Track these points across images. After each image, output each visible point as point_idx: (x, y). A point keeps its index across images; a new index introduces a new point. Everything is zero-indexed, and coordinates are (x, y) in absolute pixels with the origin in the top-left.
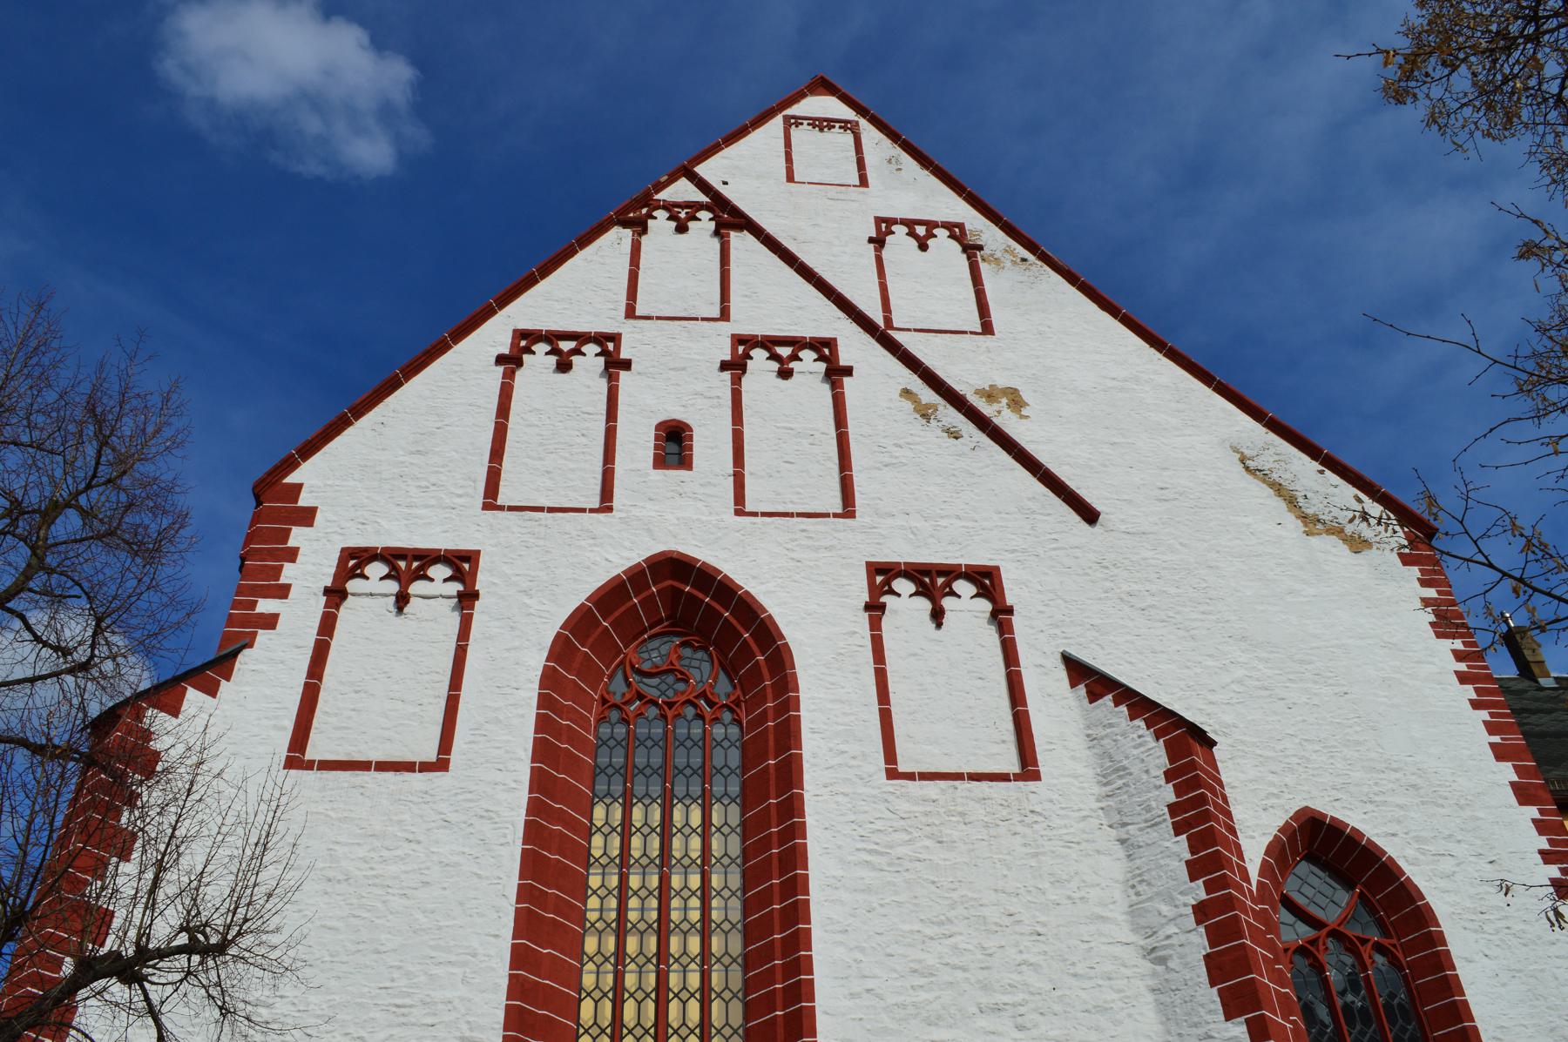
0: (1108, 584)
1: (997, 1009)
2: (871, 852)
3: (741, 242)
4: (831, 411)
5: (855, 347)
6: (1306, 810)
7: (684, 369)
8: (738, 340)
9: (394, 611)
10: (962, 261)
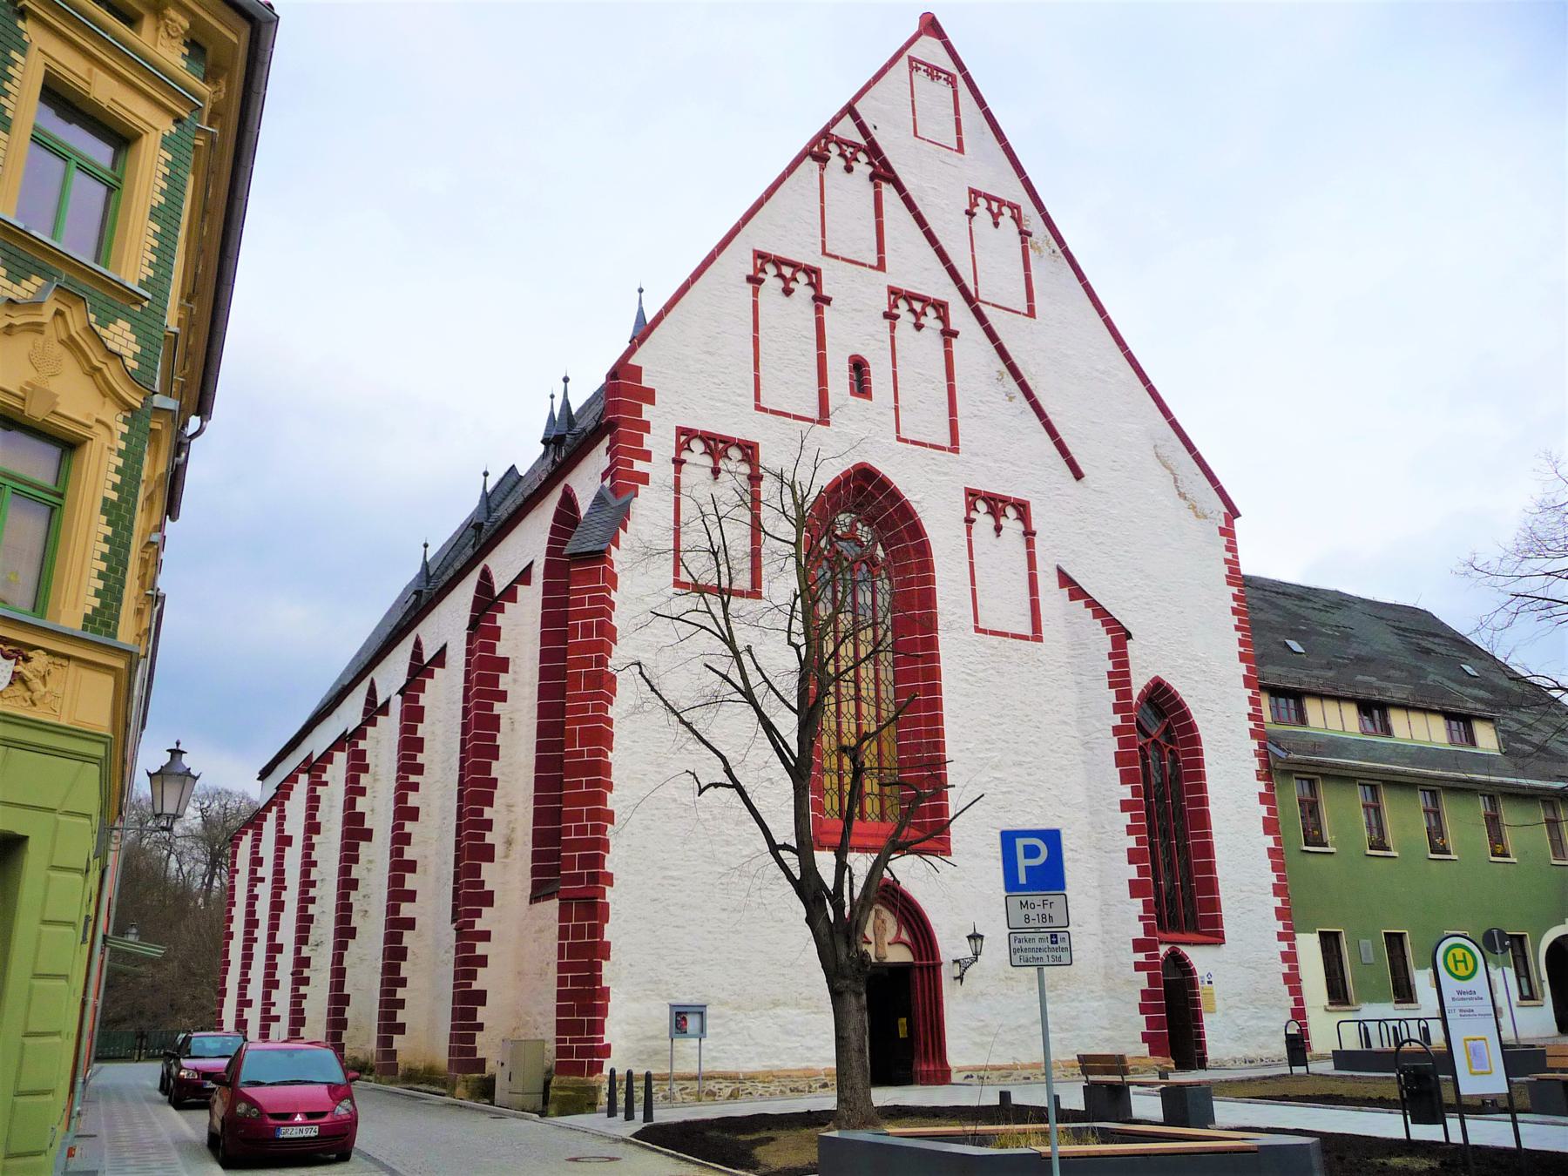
0: (1082, 524)
1: (1020, 764)
2: (968, 674)
3: (888, 191)
4: (944, 363)
5: (960, 316)
6: (1157, 677)
7: (861, 311)
8: (893, 291)
9: (712, 477)
10: (1016, 239)
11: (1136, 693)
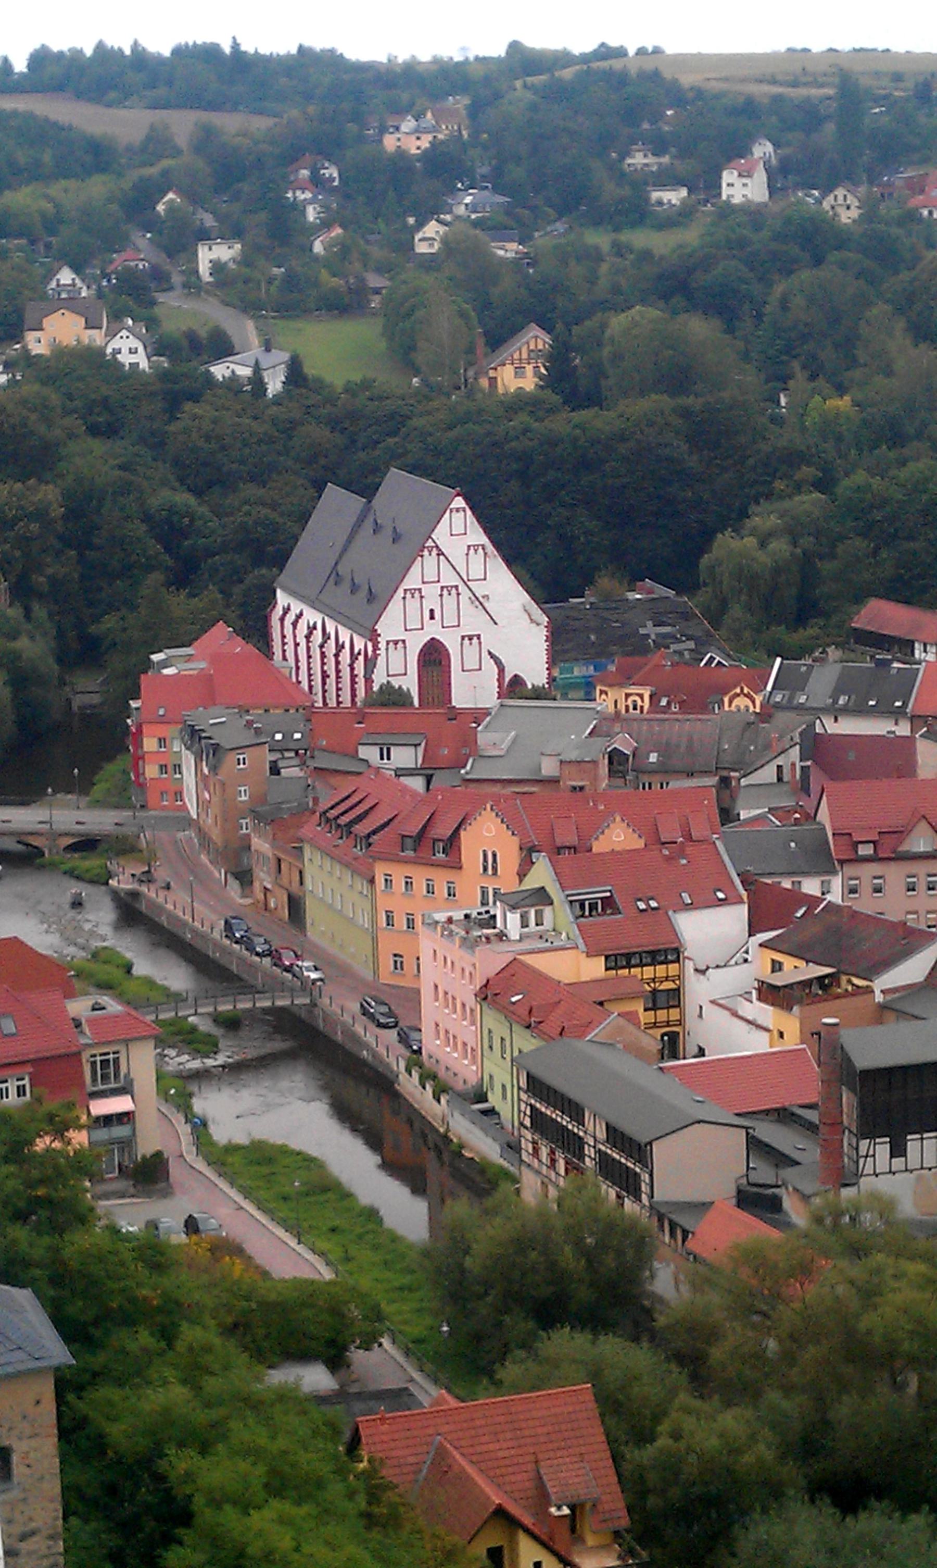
3: (442, 557)
5: (462, 588)
11: (507, 680)
